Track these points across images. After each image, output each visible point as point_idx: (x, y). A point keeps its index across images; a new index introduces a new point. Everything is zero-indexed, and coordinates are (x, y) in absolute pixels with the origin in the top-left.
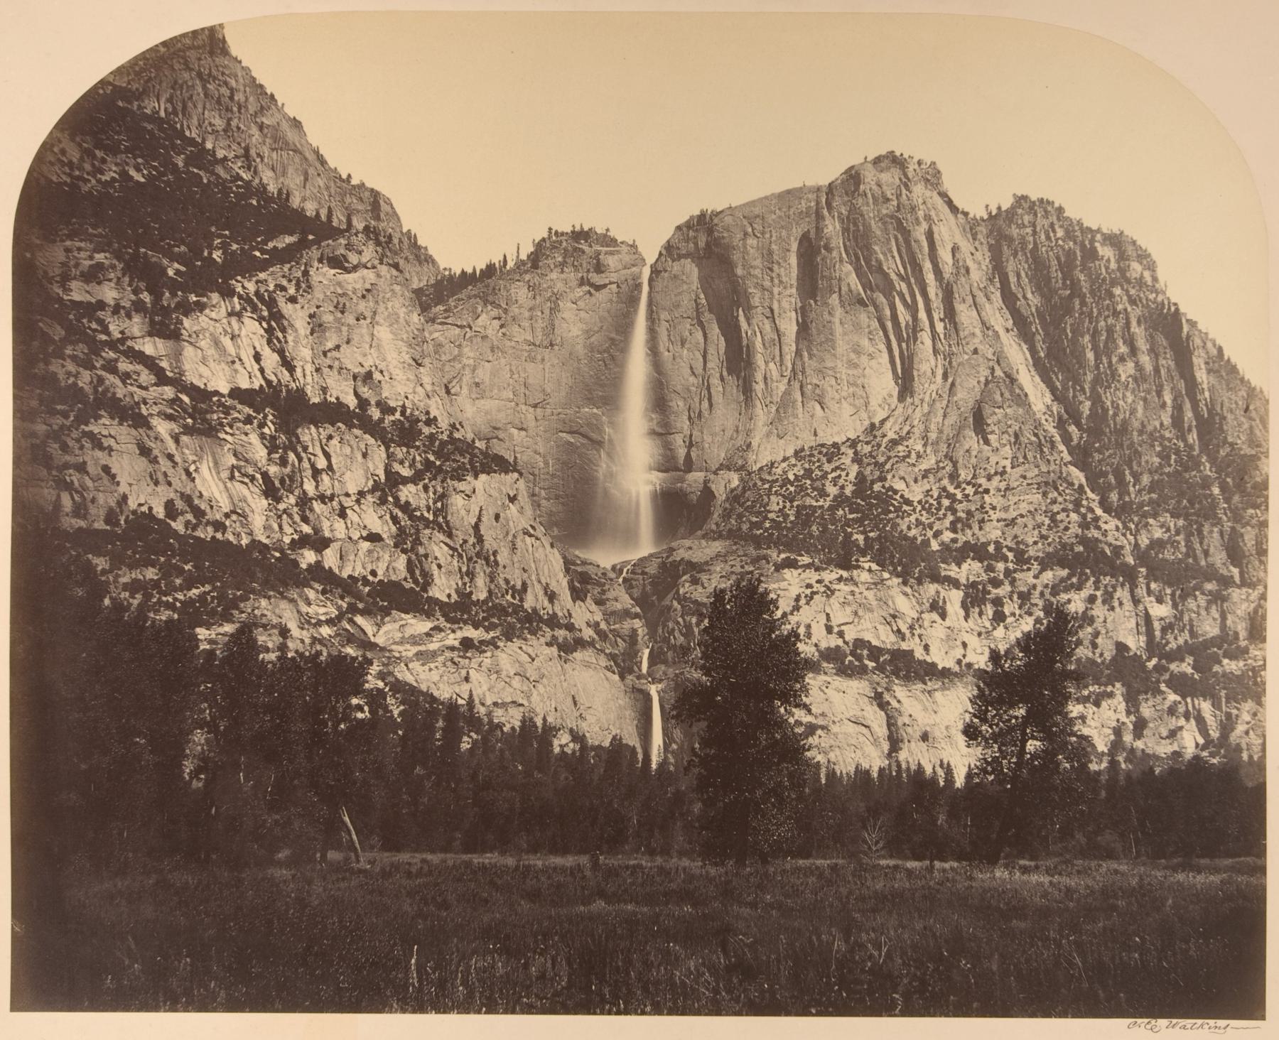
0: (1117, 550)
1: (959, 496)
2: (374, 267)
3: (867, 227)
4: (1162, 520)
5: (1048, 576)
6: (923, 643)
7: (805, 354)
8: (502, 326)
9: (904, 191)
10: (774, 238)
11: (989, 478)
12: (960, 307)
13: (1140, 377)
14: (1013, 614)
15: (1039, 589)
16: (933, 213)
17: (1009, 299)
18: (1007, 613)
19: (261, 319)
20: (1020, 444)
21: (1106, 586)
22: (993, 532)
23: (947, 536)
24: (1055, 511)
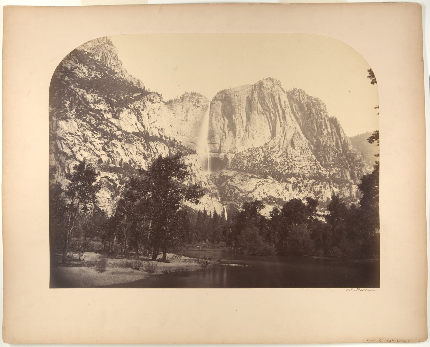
0: (325, 175)
1: (289, 161)
2: (159, 102)
3: (264, 95)
4: (335, 168)
5: (311, 181)
7: (249, 125)
8: (175, 115)
9: (273, 87)
10: (241, 97)
11: (295, 157)
12: (287, 115)
13: (328, 134)
15: (309, 184)
16: (280, 93)
17: (294, 113)
18: (302, 190)
19: (135, 114)
20: (302, 149)
21: (324, 184)
22: (297, 171)
23: (287, 171)
24: (311, 166)
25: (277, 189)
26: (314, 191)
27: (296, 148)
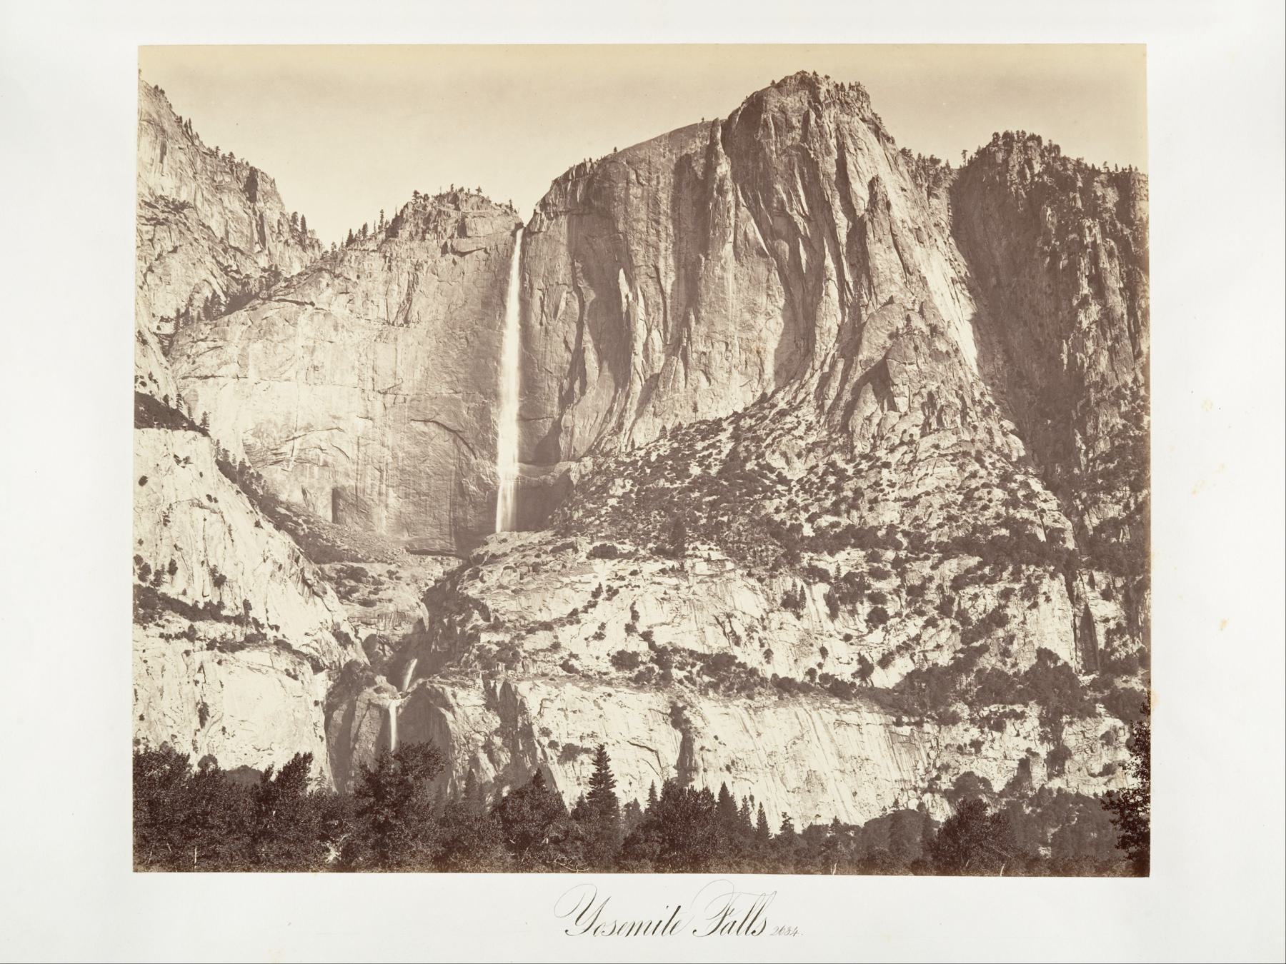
0: (1055, 535)
1: (850, 472)
4: (1119, 495)
5: (951, 568)
6: (764, 649)
7: (693, 317)
10: (662, 185)
11: (892, 450)
14: (898, 614)
15: (937, 581)
18: (891, 612)
20: (934, 406)
21: (1028, 578)
22: (889, 514)
23: (825, 521)
24: (973, 487)
25: (728, 610)
26: (963, 616)
27: (902, 403)
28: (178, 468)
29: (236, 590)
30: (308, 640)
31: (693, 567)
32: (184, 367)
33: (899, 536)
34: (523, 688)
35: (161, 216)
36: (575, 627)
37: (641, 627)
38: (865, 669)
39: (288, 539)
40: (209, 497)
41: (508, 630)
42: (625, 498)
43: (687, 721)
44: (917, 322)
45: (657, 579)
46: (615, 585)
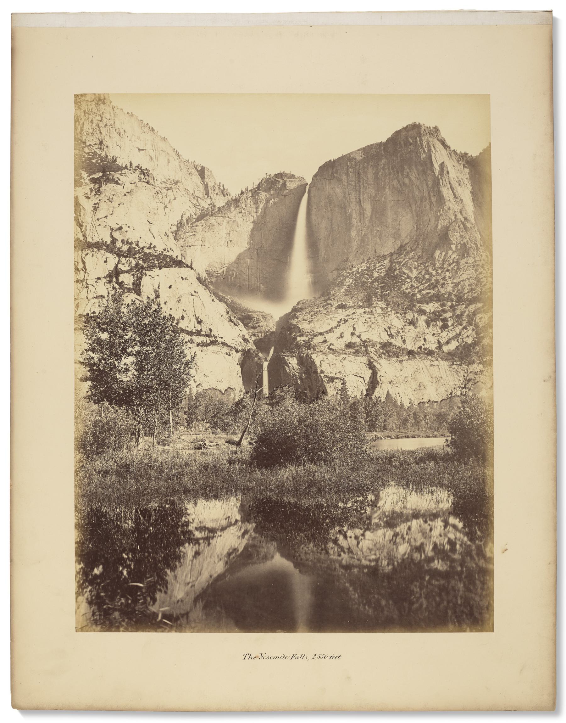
6: (403, 339)
11: (450, 265)
25: (389, 326)
28: (183, 281)
29: (206, 324)
30: (233, 341)
31: (376, 310)
32: (181, 242)
33: (453, 297)
34: (314, 356)
35: (169, 187)
36: (332, 333)
37: (357, 333)
38: (440, 347)
39: (225, 305)
40: (195, 291)
41: (307, 336)
42: (349, 286)
43: (375, 366)
44: (459, 216)
45: (362, 315)
46: (346, 318)
